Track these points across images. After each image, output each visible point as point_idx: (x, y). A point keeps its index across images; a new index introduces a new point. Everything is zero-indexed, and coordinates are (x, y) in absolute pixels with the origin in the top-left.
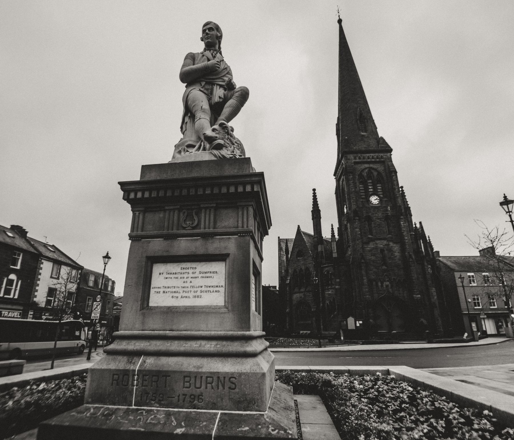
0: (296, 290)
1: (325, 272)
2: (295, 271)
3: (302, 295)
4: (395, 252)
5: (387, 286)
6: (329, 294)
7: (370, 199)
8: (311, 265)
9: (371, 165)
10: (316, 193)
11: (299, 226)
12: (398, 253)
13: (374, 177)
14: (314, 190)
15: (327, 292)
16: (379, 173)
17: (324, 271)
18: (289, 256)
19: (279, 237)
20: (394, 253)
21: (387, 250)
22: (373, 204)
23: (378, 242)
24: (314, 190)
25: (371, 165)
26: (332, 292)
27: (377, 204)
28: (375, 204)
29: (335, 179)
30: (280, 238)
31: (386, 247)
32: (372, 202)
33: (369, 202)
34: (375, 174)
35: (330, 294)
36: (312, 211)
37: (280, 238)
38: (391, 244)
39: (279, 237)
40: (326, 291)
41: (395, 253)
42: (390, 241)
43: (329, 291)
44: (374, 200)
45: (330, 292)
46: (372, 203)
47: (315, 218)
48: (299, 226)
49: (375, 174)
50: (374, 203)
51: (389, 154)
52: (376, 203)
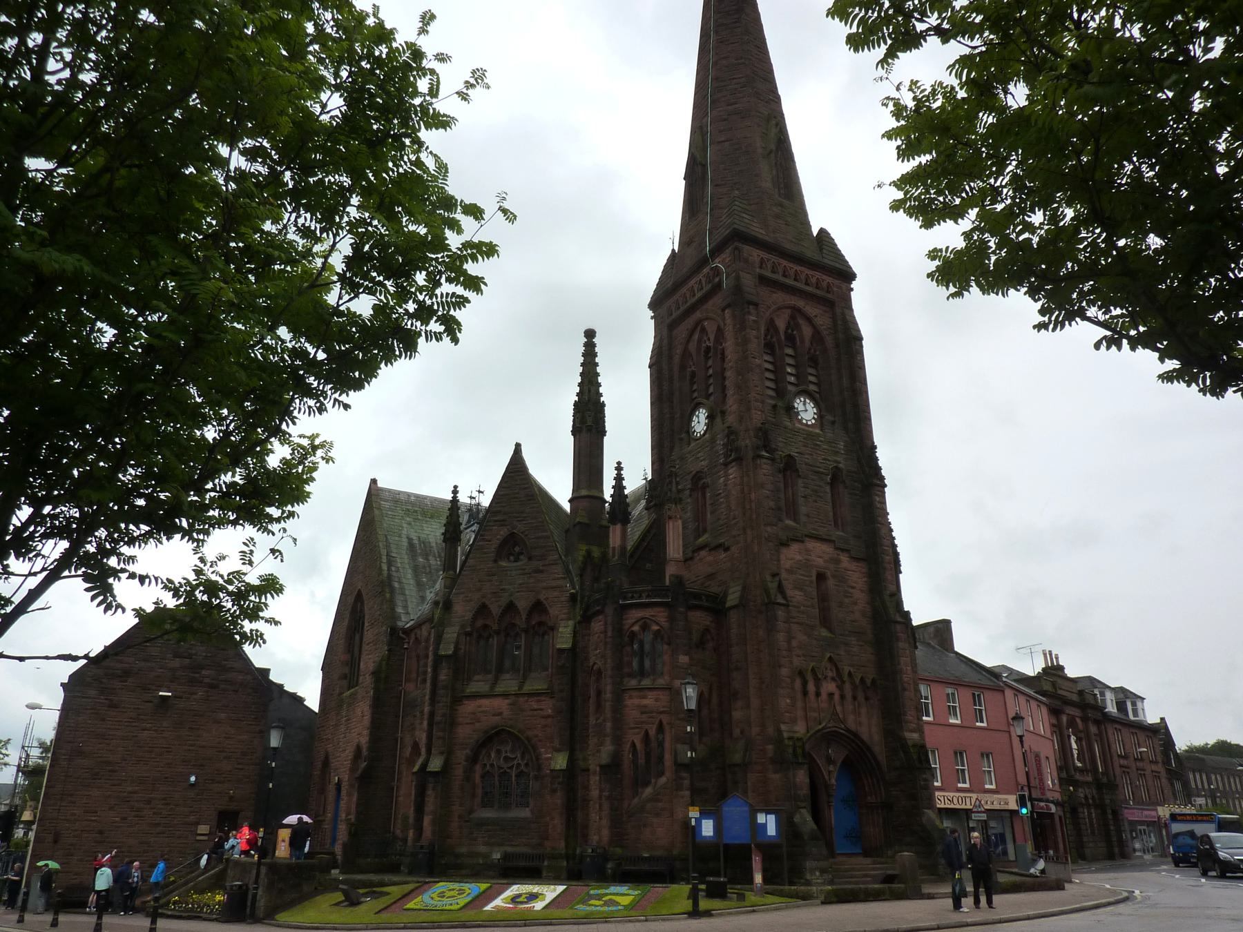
0: (478, 685)
1: (633, 625)
2: (482, 610)
3: (502, 704)
4: (853, 588)
5: (831, 695)
6: (644, 710)
8: (556, 594)
9: (800, 303)
10: (594, 345)
11: (518, 446)
12: (862, 591)
13: (802, 341)
14: (590, 334)
15: (636, 701)
16: (817, 336)
17: (630, 621)
19: (374, 481)
20: (851, 590)
21: (834, 576)
22: (800, 421)
23: (811, 544)
24: (590, 334)
25: (800, 303)
26: (657, 700)
28: (807, 425)
29: (652, 318)
33: (790, 411)
34: (807, 331)
35: (645, 706)
36: (576, 404)
37: (380, 484)
38: (844, 558)
40: (631, 697)
42: (843, 550)
43: (644, 697)
45: (645, 702)
47: (589, 429)
48: (518, 446)
49: (807, 331)
51: (844, 286)
52: (809, 423)
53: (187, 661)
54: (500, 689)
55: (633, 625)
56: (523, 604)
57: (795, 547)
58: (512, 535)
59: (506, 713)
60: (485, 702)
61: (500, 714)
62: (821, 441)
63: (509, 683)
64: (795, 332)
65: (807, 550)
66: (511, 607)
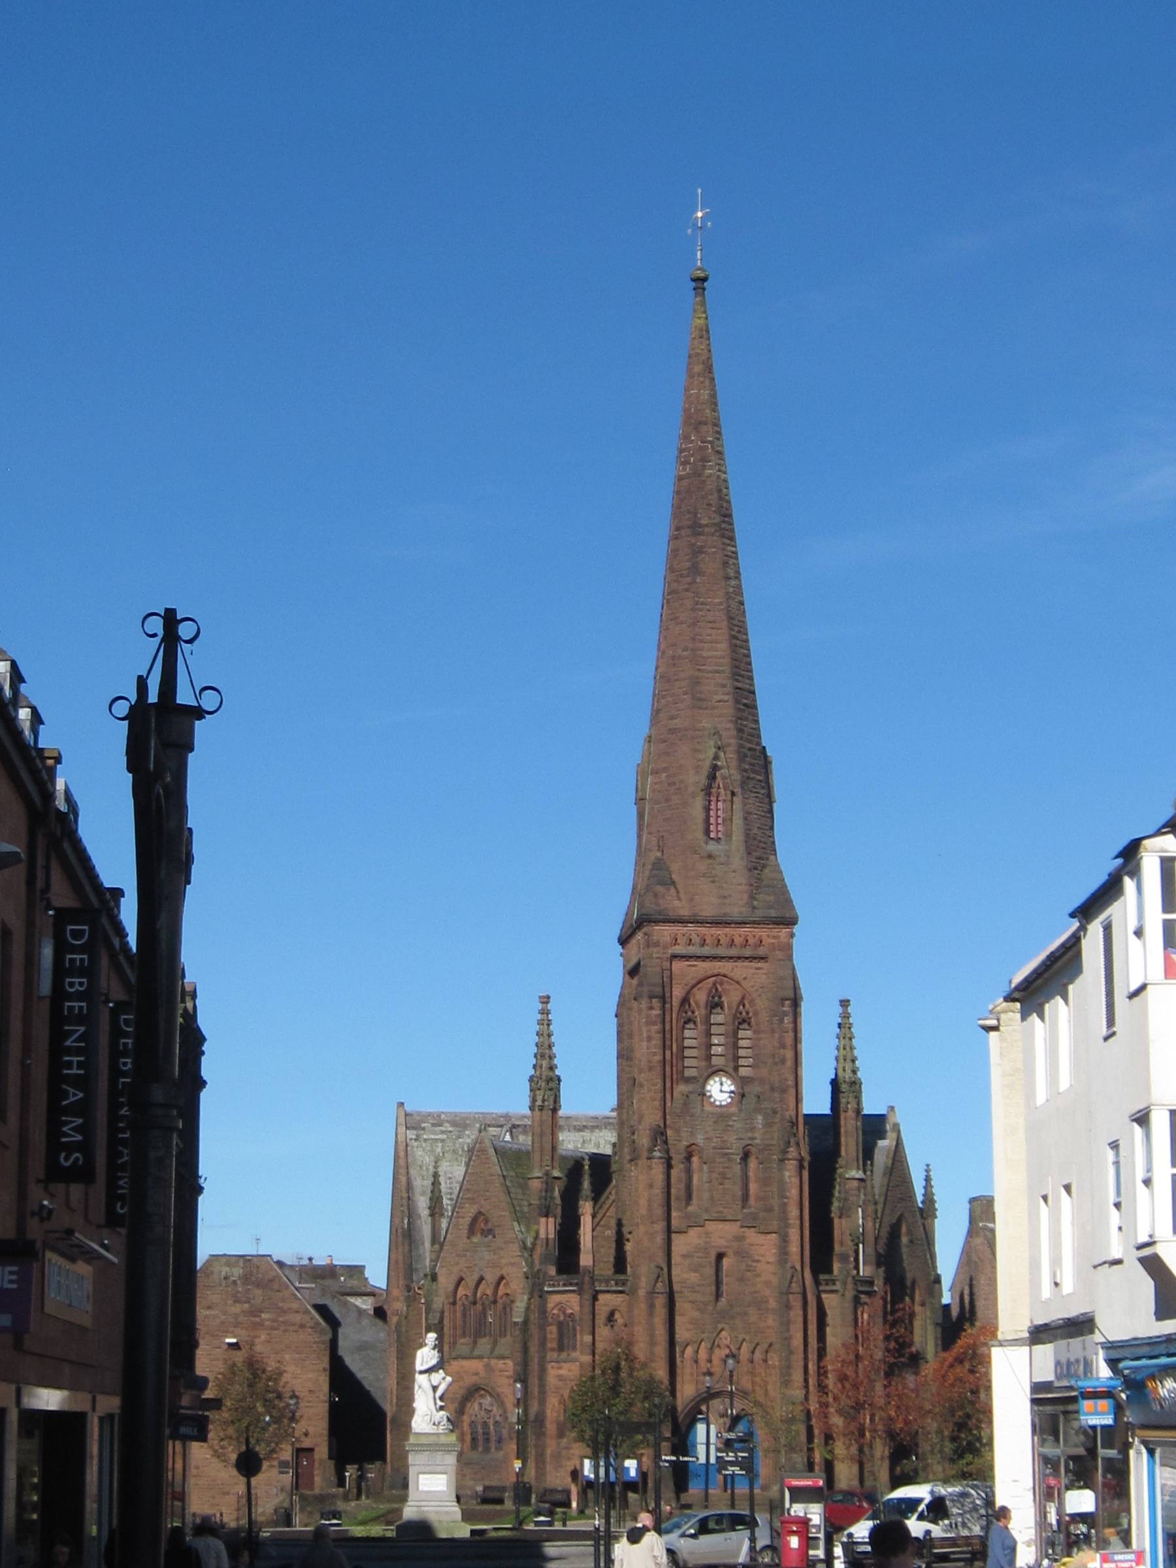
1: (553, 1309)
4: (758, 1261)
6: (561, 1378)
7: (708, 1088)
18: (444, 1223)
20: (754, 1264)
22: (713, 1104)
23: (711, 1226)
27: (729, 1105)
28: (721, 1106)
30: (408, 1108)
31: (735, 1244)
32: (711, 1096)
34: (730, 998)
35: (561, 1376)
38: (752, 1236)
39: (401, 1104)
41: (759, 1264)
43: (560, 1368)
44: (720, 1090)
45: (561, 1372)
46: (712, 1100)
50: (717, 1103)
51: (784, 932)
53: (246, 1306)
54: (476, 1353)
55: (553, 1309)
56: (491, 1277)
57: (693, 1232)
58: (480, 1213)
59: (482, 1373)
60: (465, 1363)
61: (477, 1374)
62: (734, 1121)
63: (484, 1344)
64: (723, 999)
65: (707, 1234)
66: (481, 1279)
